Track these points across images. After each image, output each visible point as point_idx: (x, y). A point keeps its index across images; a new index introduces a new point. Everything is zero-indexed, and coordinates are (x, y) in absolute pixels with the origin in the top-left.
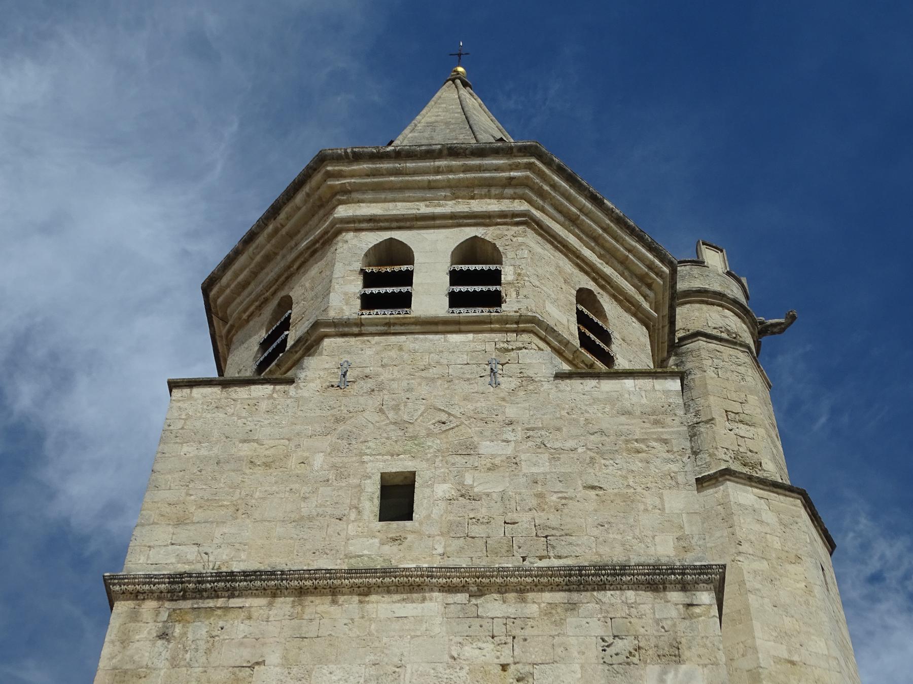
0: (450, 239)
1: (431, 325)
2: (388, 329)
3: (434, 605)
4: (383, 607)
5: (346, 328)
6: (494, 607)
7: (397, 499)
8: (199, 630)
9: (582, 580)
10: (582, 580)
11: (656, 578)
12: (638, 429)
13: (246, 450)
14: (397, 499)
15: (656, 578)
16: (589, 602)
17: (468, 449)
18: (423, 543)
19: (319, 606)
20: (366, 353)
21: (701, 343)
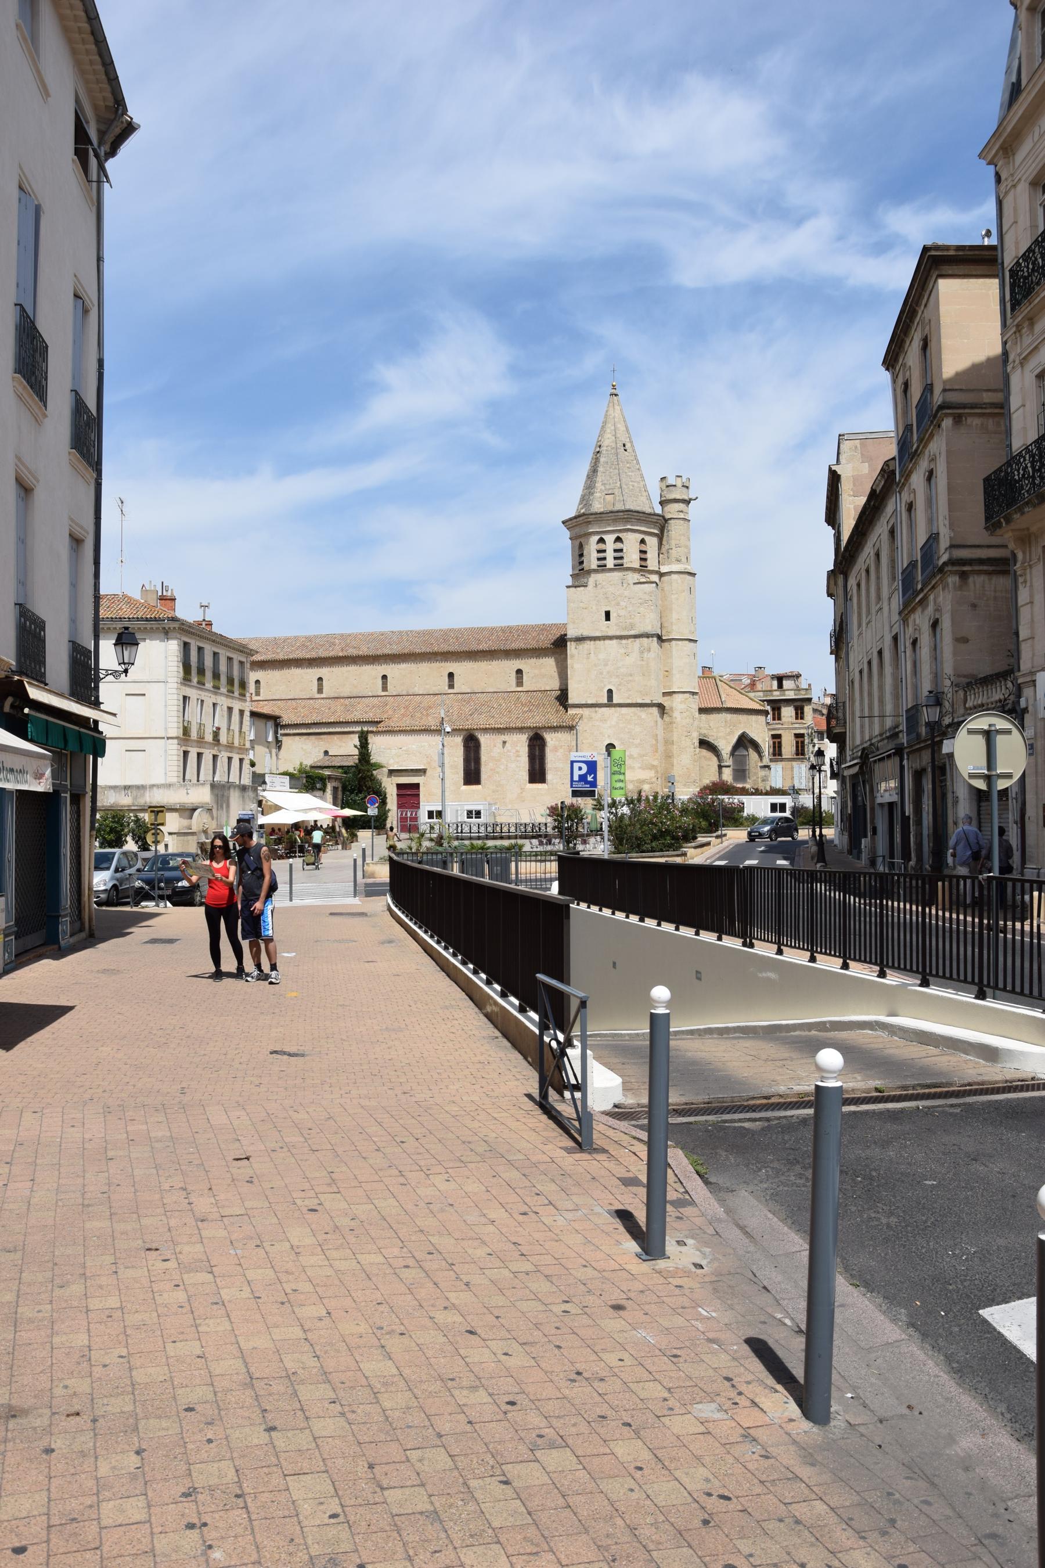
0: (614, 536)
1: (611, 570)
2: (603, 571)
3: (615, 641)
4: (607, 642)
5: (595, 571)
6: (624, 641)
7: (608, 616)
8: (581, 647)
9: (636, 637)
10: (636, 637)
11: (647, 636)
12: (647, 597)
13: (581, 605)
14: (608, 616)
15: (647, 636)
16: (638, 640)
17: (618, 604)
18: (611, 628)
19: (598, 642)
20: (599, 577)
21: (672, 521)
